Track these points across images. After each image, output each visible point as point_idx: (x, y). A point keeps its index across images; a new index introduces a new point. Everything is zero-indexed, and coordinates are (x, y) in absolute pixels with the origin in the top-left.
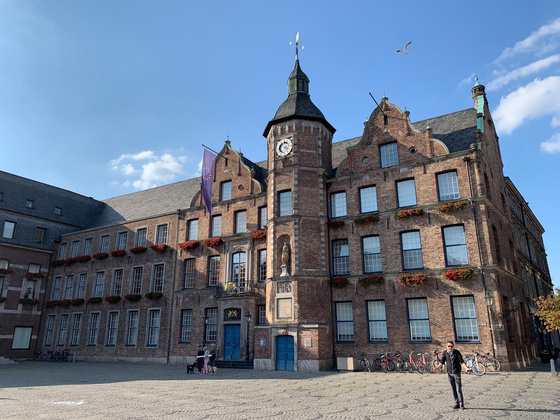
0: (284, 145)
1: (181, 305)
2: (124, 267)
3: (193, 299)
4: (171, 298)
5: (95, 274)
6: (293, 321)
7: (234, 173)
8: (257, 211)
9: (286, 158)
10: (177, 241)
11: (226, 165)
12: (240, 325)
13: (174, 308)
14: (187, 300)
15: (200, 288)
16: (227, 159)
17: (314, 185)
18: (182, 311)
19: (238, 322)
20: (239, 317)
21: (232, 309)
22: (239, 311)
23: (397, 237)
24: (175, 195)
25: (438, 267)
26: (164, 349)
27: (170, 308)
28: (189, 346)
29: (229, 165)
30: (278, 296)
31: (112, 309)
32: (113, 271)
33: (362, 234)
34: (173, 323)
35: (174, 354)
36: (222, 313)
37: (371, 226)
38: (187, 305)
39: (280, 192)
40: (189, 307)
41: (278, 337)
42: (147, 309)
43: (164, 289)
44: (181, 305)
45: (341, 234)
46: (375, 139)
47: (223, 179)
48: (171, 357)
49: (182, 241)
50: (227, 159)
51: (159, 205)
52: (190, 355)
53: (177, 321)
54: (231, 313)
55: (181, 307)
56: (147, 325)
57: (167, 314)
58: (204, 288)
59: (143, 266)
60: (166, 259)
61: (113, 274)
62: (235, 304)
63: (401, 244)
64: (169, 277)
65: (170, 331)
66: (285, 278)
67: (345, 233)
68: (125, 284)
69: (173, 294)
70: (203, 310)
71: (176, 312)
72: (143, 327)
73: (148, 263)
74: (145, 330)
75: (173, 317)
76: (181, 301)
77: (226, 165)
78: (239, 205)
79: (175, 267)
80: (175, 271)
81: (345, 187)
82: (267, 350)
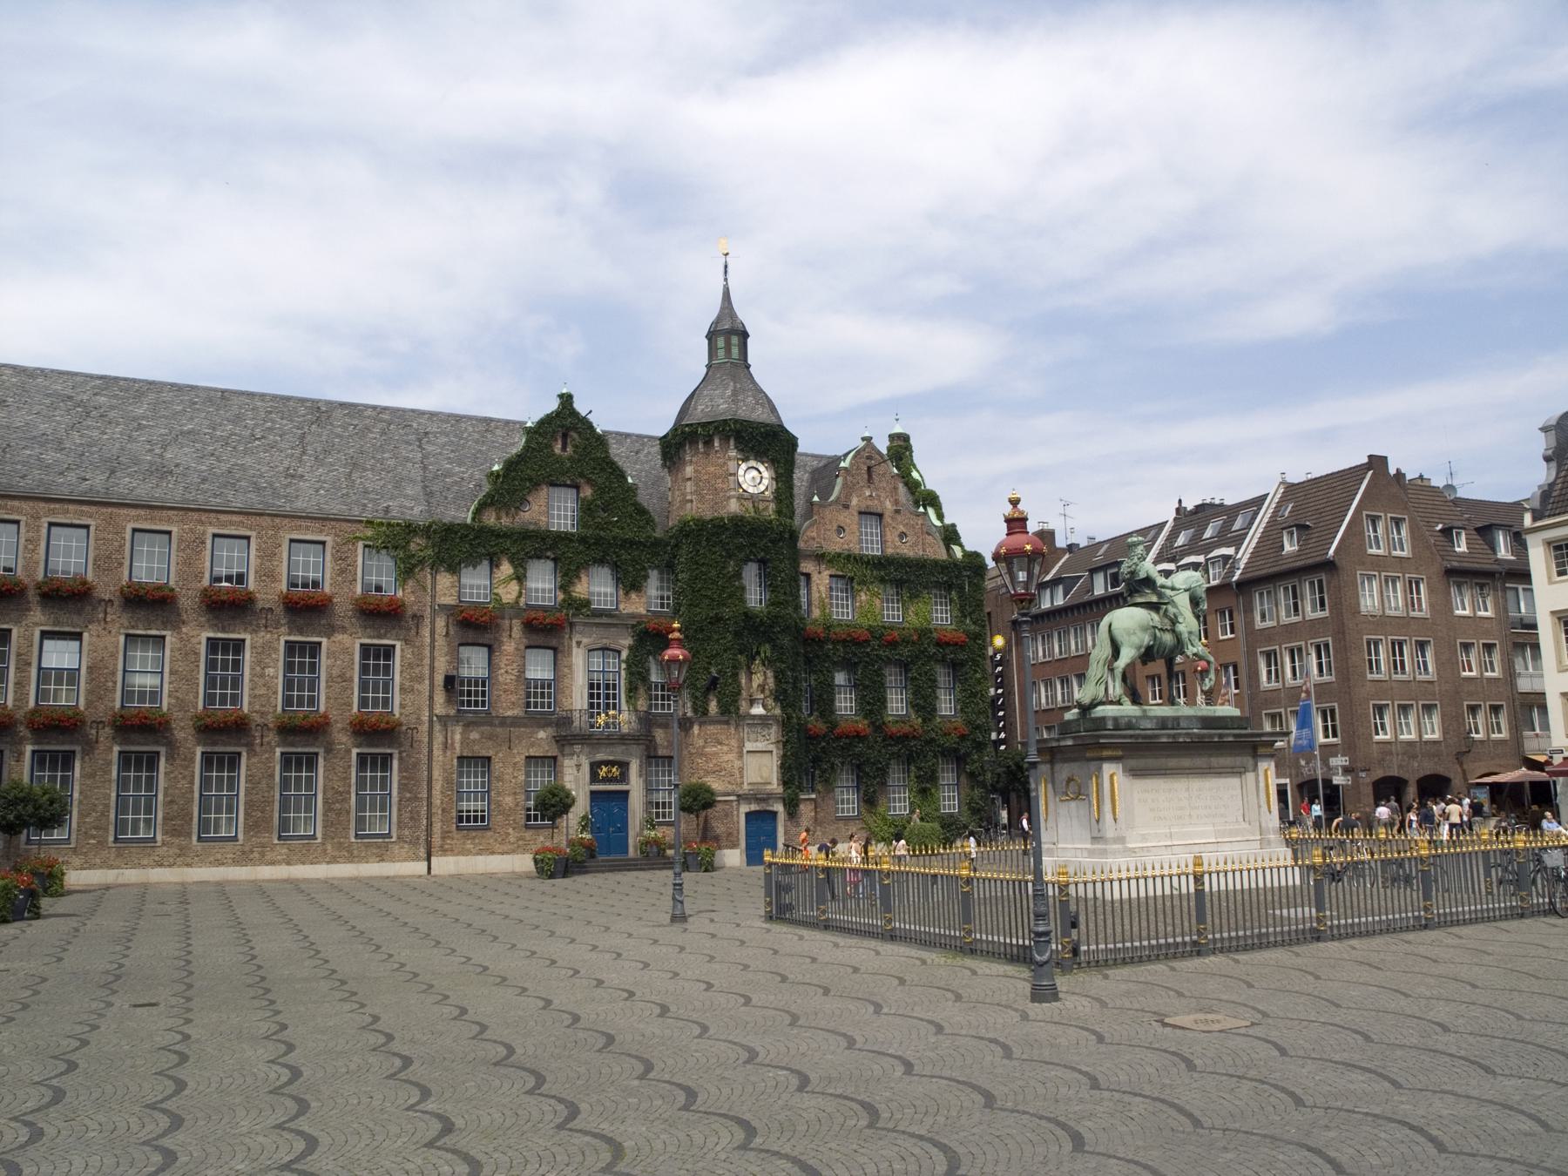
0: (754, 473)
1: (457, 746)
3: (490, 737)
4: (425, 727)
5: (122, 639)
6: (775, 786)
10: (433, 597)
12: (627, 793)
13: (437, 752)
14: (474, 735)
15: (509, 713)
18: (460, 758)
20: (623, 778)
21: (606, 763)
22: (624, 766)
26: (414, 842)
27: (425, 751)
28: (489, 833)
30: (749, 746)
31: (214, 744)
32: (204, 642)
34: (437, 787)
35: (444, 851)
38: (476, 748)
40: (484, 753)
41: (747, 814)
42: (349, 751)
43: (402, 706)
44: (457, 746)
46: (854, 501)
48: (433, 859)
49: (449, 600)
52: (493, 853)
53: (448, 781)
55: (458, 752)
56: (353, 789)
57: (416, 765)
58: (522, 714)
59: (324, 641)
61: (203, 649)
62: (616, 754)
64: (420, 679)
65: (429, 805)
66: (760, 717)
68: (261, 682)
69: (431, 721)
70: (520, 759)
71: (442, 764)
72: (338, 792)
73: (339, 637)
74: (347, 800)
75: (436, 774)
76: (458, 737)
79: (433, 659)
82: (730, 834)
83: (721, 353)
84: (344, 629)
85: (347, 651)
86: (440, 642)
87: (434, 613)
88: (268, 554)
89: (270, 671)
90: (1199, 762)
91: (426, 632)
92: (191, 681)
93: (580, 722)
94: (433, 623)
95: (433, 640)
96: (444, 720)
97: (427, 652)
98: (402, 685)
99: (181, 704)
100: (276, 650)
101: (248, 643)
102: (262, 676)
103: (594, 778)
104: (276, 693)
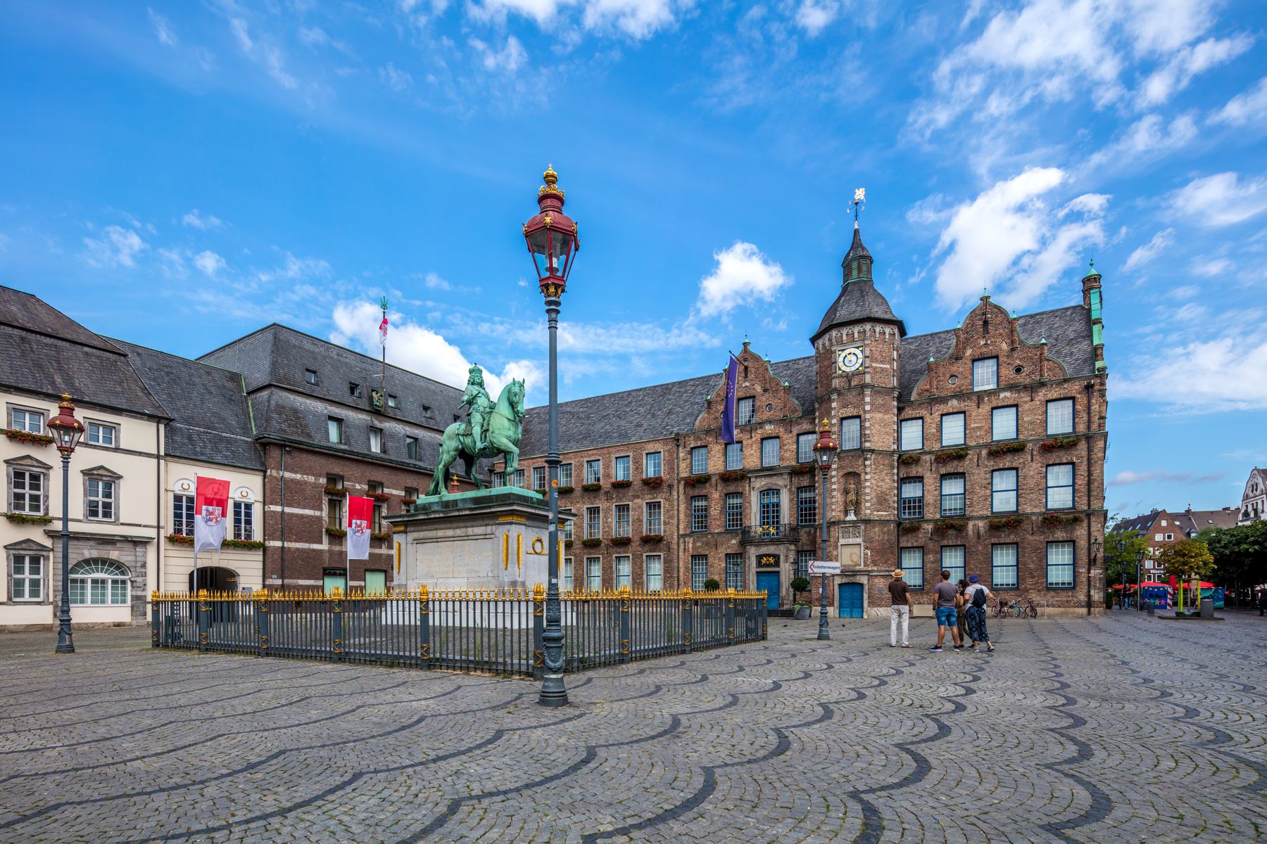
2: (601, 504)
7: (758, 388)
8: (795, 439)
9: (848, 377)
11: (746, 376)
16: (746, 368)
17: (886, 412)
23: (988, 476)
24: (642, 410)
25: (1037, 510)
29: (751, 376)
33: (943, 471)
37: (955, 463)
39: (843, 419)
45: (914, 470)
47: (741, 394)
50: (746, 368)
51: (623, 423)
63: (991, 484)
64: (671, 517)
67: (920, 470)
77: (746, 376)
78: (769, 428)
81: (923, 412)
84: (638, 497)
85: (640, 507)
87: (679, 482)
88: (607, 466)
90: (458, 532)
91: (675, 493)
92: (582, 527)
99: (578, 537)
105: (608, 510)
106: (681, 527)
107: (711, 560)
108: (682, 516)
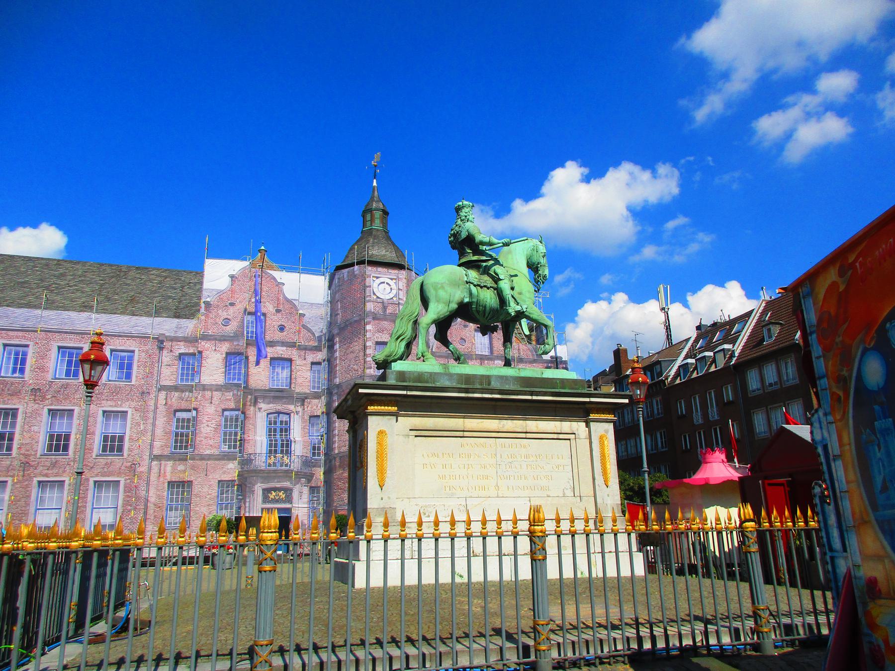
19: (288, 506)
20: (289, 499)
21: (275, 489)
22: (288, 491)
36: (261, 492)
54: (274, 494)
60: (134, 404)
64: (143, 433)
79: (155, 419)
80: (154, 425)
83: (368, 223)
86: (162, 408)
89: (36, 428)
93: (261, 462)
94: (157, 397)
95: (156, 408)
96: (158, 458)
97: (151, 415)
98: (131, 436)
100: (40, 415)
101: (20, 412)
102: (29, 431)
103: (266, 499)
104: (37, 442)
105: (36, 413)
106: (157, 444)
107: (196, 489)
108: (159, 432)
